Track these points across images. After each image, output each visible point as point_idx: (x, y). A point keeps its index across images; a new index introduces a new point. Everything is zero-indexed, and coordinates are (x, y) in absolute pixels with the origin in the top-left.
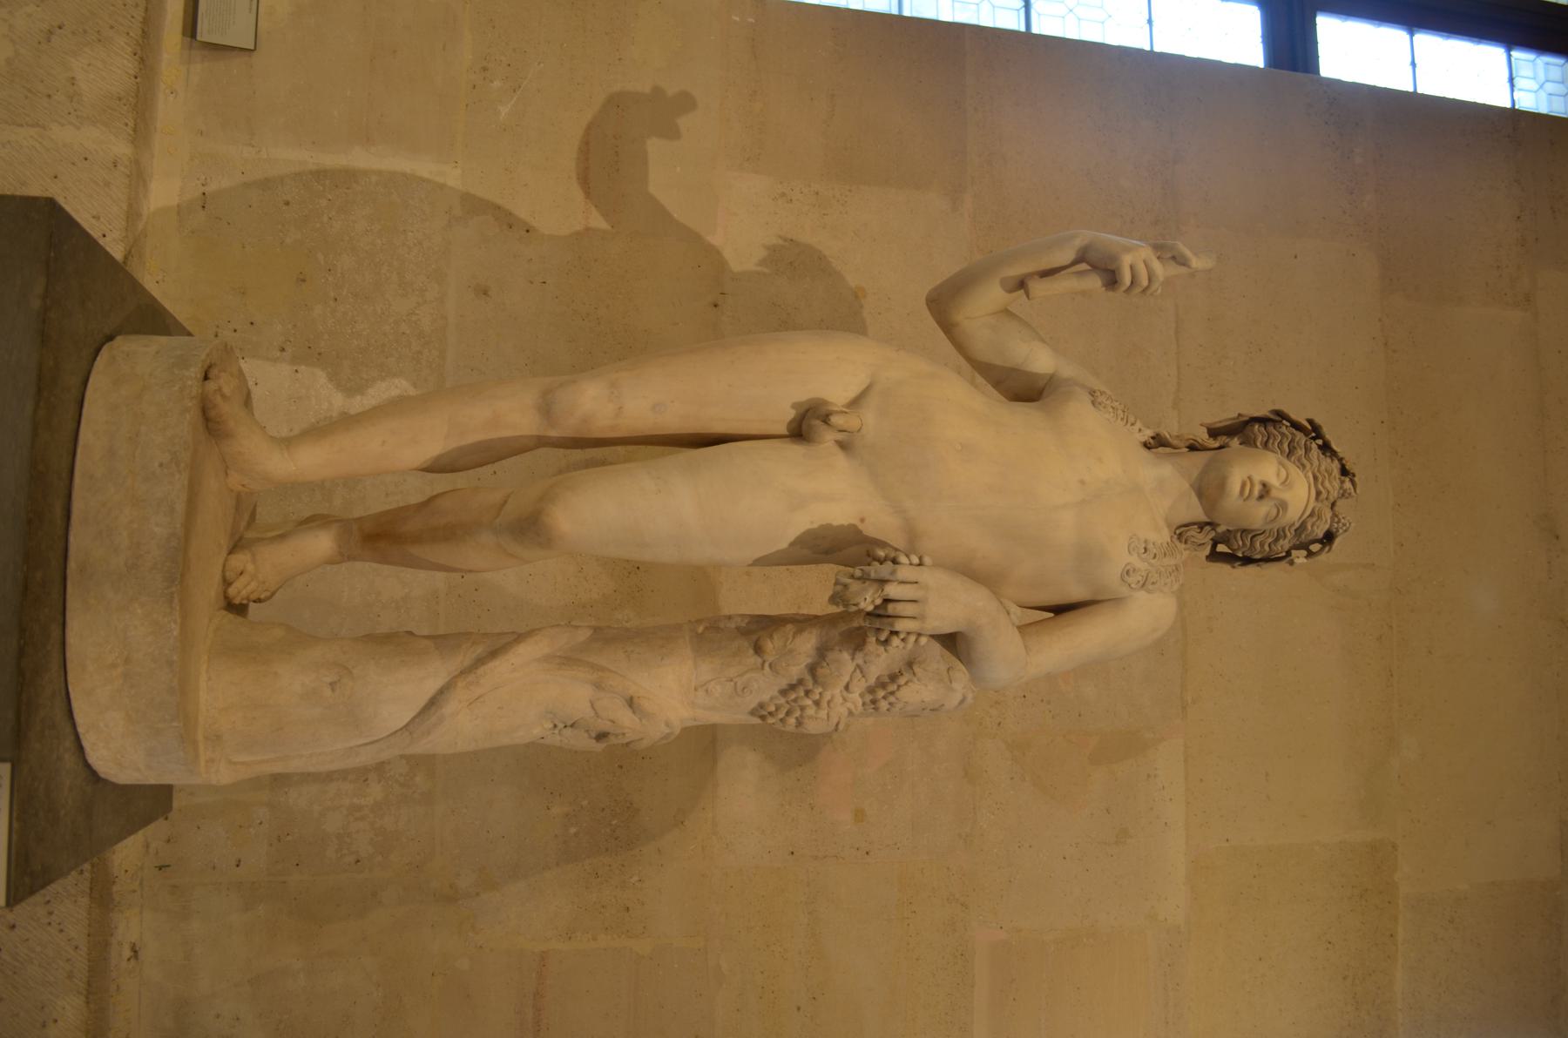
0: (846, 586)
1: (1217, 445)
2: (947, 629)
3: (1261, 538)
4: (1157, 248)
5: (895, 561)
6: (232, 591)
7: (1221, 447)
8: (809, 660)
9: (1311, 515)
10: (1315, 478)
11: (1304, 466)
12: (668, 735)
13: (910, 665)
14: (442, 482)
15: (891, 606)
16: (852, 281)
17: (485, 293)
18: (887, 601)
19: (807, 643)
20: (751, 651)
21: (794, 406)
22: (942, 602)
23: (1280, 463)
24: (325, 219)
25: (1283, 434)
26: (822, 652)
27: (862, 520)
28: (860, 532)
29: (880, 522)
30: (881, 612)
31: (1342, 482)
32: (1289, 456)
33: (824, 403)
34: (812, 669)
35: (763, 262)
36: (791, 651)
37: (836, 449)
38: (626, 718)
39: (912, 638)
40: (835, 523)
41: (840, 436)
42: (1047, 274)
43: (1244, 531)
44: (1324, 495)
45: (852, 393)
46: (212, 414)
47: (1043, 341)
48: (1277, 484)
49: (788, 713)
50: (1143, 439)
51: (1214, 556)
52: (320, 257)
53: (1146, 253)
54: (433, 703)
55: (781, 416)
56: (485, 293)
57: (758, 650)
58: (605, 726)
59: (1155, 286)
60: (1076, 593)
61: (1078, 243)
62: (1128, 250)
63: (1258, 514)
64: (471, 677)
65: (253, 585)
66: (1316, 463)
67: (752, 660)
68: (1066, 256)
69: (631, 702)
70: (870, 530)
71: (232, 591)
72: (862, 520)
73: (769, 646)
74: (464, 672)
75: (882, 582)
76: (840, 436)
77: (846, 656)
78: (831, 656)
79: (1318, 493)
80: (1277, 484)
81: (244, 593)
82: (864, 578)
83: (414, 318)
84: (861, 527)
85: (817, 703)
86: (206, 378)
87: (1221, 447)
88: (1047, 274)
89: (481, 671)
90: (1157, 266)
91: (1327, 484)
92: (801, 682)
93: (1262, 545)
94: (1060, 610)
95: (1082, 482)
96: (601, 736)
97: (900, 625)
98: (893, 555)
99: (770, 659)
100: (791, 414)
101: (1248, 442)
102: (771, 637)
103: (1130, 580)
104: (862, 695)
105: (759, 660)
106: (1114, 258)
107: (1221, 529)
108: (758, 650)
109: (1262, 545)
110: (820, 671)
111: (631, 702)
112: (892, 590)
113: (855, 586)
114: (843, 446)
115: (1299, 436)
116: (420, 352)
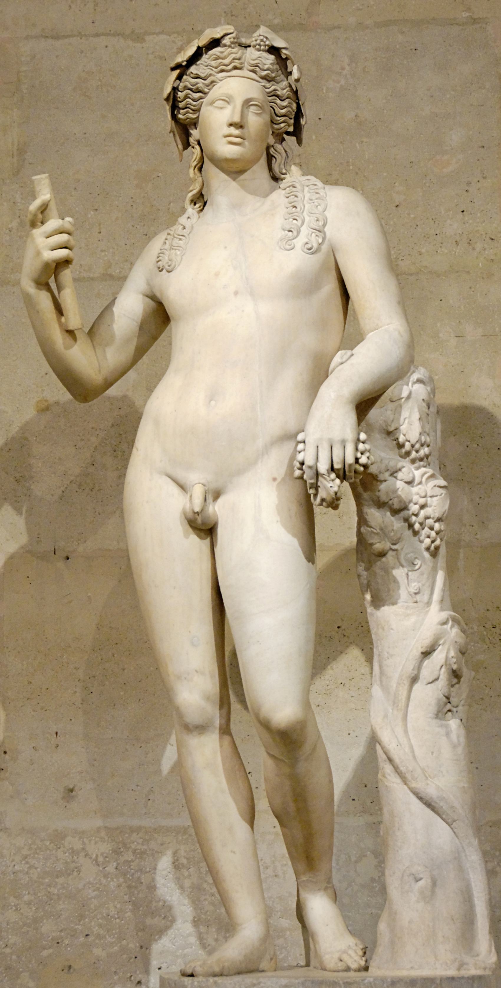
0: (323, 500)
1: (197, 147)
2: (352, 417)
3: (278, 110)
4: (33, 225)
5: (302, 464)
6: (354, 966)
7: (199, 144)
8: (388, 514)
9: (254, 72)
10: (222, 71)
11: (213, 82)
12: (454, 620)
13: (389, 433)
14: (262, 805)
15: (336, 466)
16: (30, 413)
17: (72, 791)
18: (332, 469)
19: (375, 515)
20: (384, 559)
21: (186, 536)
22: (330, 431)
23: (212, 103)
24: (8, 950)
25: (186, 97)
26: (380, 505)
27: (275, 479)
28: (283, 480)
29: (274, 464)
30: (341, 473)
31: (225, 46)
32: (205, 93)
33: (184, 513)
34: (395, 512)
35: (18, 511)
36: (381, 529)
37: (220, 500)
38: (439, 656)
39: (361, 446)
40: (277, 502)
41: (210, 499)
42: (59, 310)
43: (272, 122)
44: (237, 63)
45: (175, 490)
46: (217, 969)
47: (113, 302)
48: (230, 100)
49: (432, 528)
50: (196, 215)
51: (297, 132)
52: (45, 953)
53: (38, 233)
54: (429, 804)
55: (197, 545)
56: (72, 791)
57: (382, 554)
58: (444, 675)
59: (68, 226)
60: (330, 287)
61: (31, 289)
62: (38, 253)
63: (255, 121)
64: (409, 776)
65: (351, 952)
66: (208, 71)
67: (390, 558)
68: (44, 300)
69: (427, 654)
70: (281, 472)
71: (354, 966)
72: (275, 479)
73: (378, 546)
74: (405, 781)
75: (317, 474)
76: (210, 499)
77: (383, 487)
78: (384, 498)
79: (235, 68)
80: (230, 100)
81: (357, 958)
82: (316, 487)
83: (101, 859)
84: (279, 480)
85: (423, 507)
86: (192, 975)
87: (199, 144)
88: (59, 310)
89: (403, 769)
90: (53, 224)
91: (226, 61)
92: (406, 520)
93: (284, 107)
94: (345, 296)
95: (236, 293)
96: (456, 675)
97: (350, 460)
98: (298, 465)
99: (388, 545)
100: (194, 538)
101: (195, 124)
102: (372, 544)
103: (315, 246)
104: (418, 468)
105: (390, 553)
106: (47, 265)
107: (271, 140)
108: (382, 554)
109: (284, 107)
110: (396, 506)
111: (427, 654)
112: (323, 467)
113: (322, 493)
114: (217, 495)
115: (188, 80)
116: (134, 852)
